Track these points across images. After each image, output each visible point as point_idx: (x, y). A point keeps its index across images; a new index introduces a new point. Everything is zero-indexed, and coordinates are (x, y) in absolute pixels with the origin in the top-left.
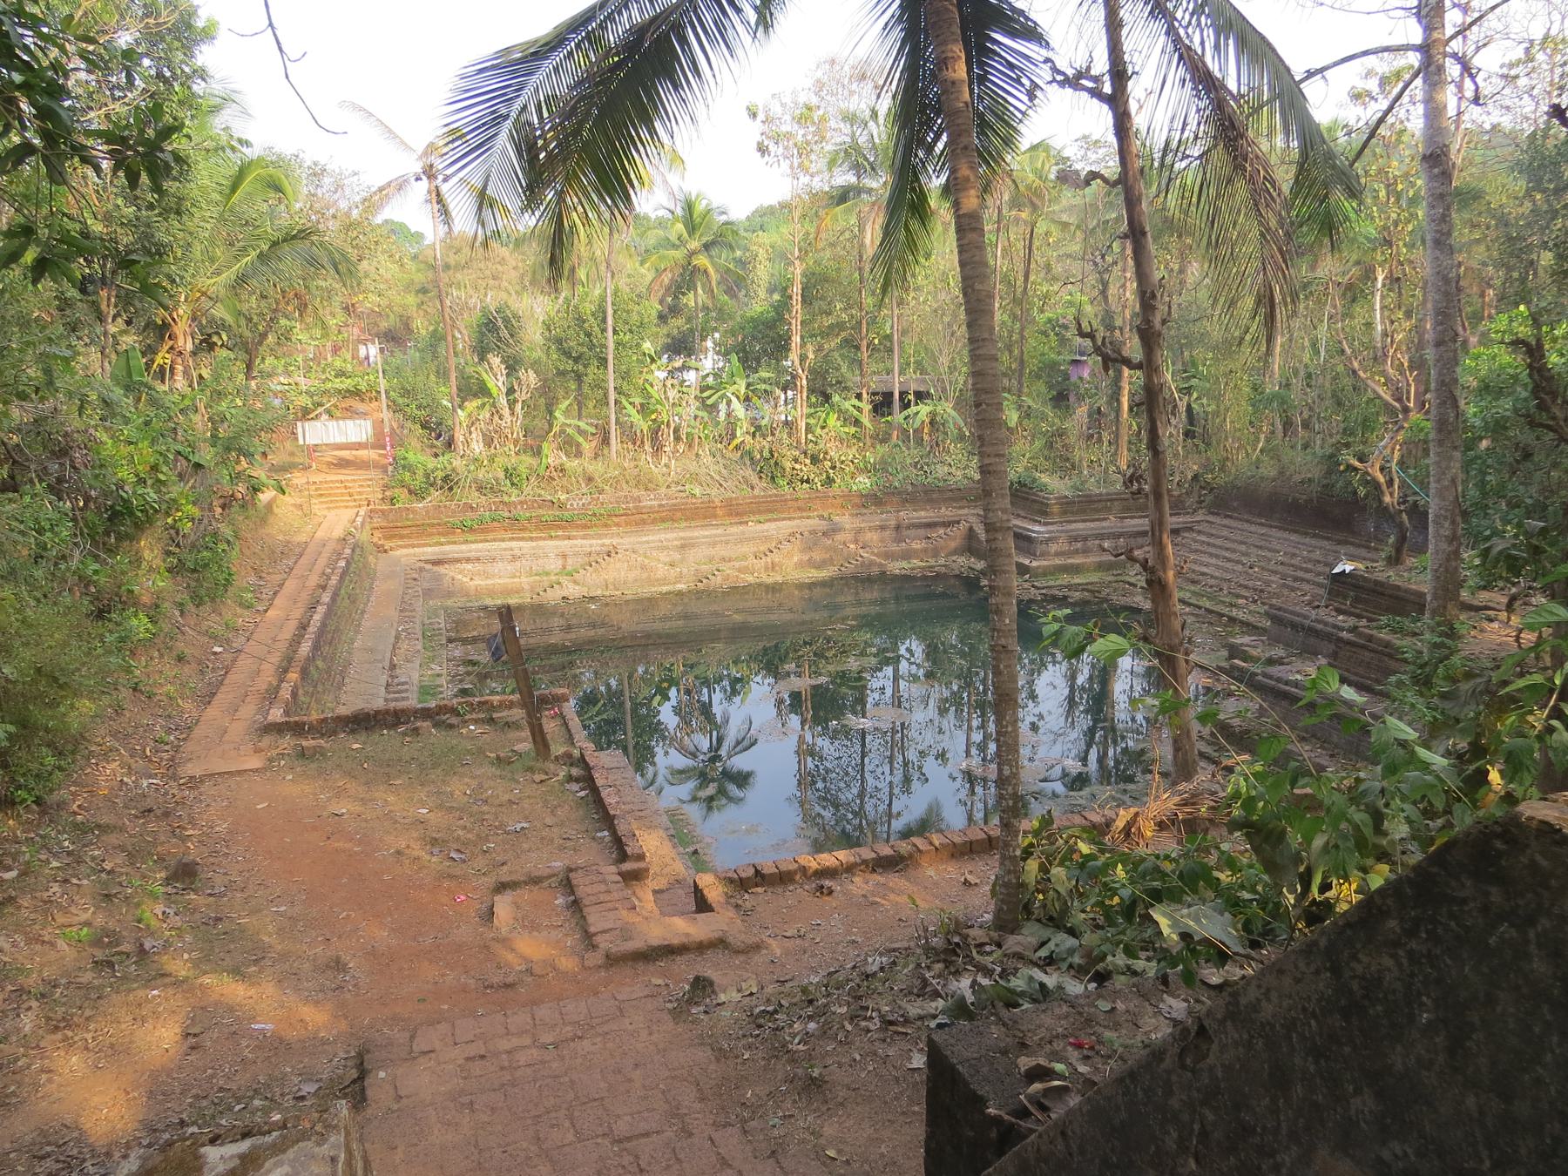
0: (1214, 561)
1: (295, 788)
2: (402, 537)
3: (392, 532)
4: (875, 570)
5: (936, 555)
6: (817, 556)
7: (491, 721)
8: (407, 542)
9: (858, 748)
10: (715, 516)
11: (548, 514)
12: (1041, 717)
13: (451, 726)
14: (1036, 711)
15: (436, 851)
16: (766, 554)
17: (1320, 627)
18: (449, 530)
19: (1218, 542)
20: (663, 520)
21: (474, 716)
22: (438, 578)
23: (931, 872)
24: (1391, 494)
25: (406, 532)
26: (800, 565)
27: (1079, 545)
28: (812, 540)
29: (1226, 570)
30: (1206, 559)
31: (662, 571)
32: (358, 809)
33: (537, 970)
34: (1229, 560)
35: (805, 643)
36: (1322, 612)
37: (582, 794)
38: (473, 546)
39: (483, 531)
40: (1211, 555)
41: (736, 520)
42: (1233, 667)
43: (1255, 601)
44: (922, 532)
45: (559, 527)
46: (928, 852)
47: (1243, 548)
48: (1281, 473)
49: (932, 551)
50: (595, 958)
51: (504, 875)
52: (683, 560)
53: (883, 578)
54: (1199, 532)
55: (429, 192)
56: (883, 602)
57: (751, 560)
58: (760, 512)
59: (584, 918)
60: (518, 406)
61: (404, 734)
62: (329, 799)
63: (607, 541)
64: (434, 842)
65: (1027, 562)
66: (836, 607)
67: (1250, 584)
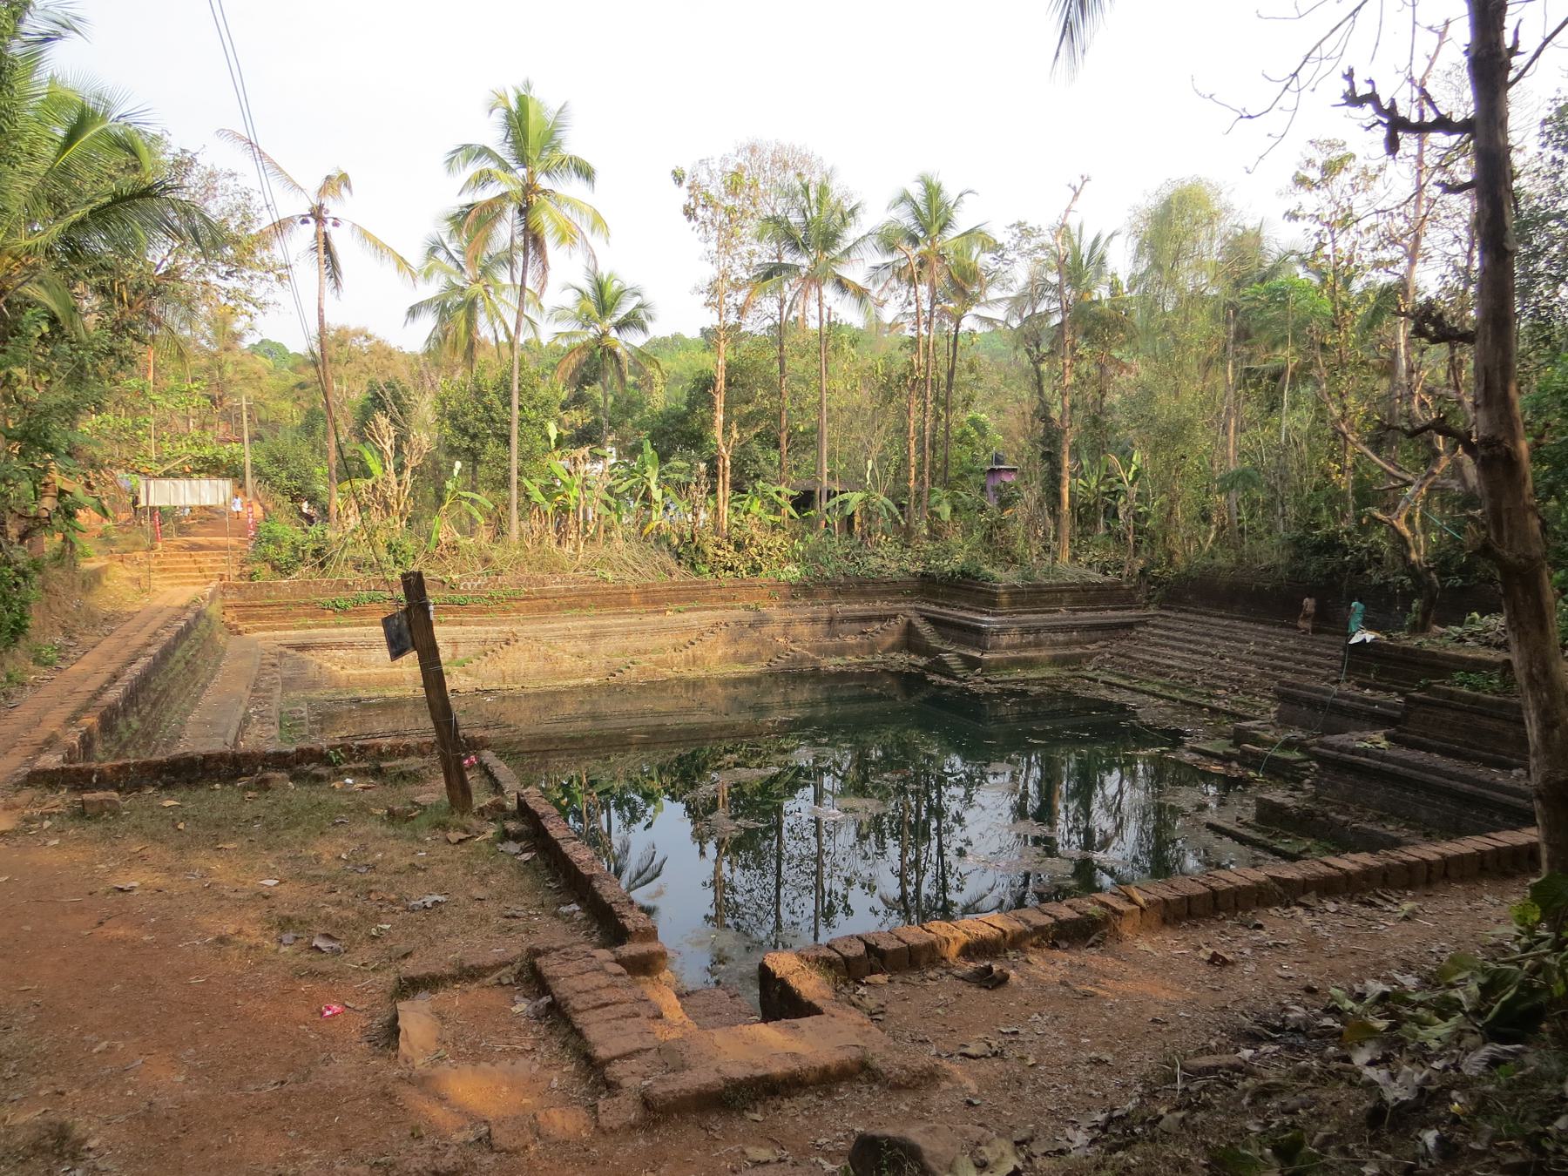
0: (1177, 653)
1: (61, 855)
2: (260, 618)
3: (248, 612)
4: (808, 666)
5: (872, 652)
6: (744, 648)
7: (378, 773)
8: (266, 623)
9: (771, 879)
10: (629, 604)
12: (969, 843)
13: (319, 779)
14: (963, 836)
15: (288, 937)
16: (689, 649)
17: (1346, 702)
18: (319, 611)
19: (1178, 635)
20: (570, 606)
21: (353, 766)
22: (302, 665)
23: (1143, 945)
24: (1418, 551)
26: (724, 659)
27: (1031, 637)
28: (739, 632)
29: (1195, 662)
30: (1169, 652)
31: (568, 663)
32: (159, 880)
33: (502, 1138)
34: (1194, 652)
35: (726, 751)
36: (1344, 687)
37: (526, 856)
38: (346, 630)
40: (1173, 648)
41: (653, 608)
42: (1245, 753)
43: (1235, 692)
44: (856, 626)
45: (450, 611)
46: (1131, 913)
47: (1208, 640)
48: (1240, 561)
49: (868, 647)
50: (620, 1111)
51: (411, 968)
52: (592, 651)
53: (816, 675)
54: (1155, 626)
55: (316, 236)
56: (813, 704)
57: (670, 653)
58: (680, 601)
59: (579, 1033)
60: (407, 474)
61: (246, 789)
62: (112, 871)
63: (506, 629)
64: (285, 923)
65: (978, 655)
66: (760, 709)
67: (1225, 674)
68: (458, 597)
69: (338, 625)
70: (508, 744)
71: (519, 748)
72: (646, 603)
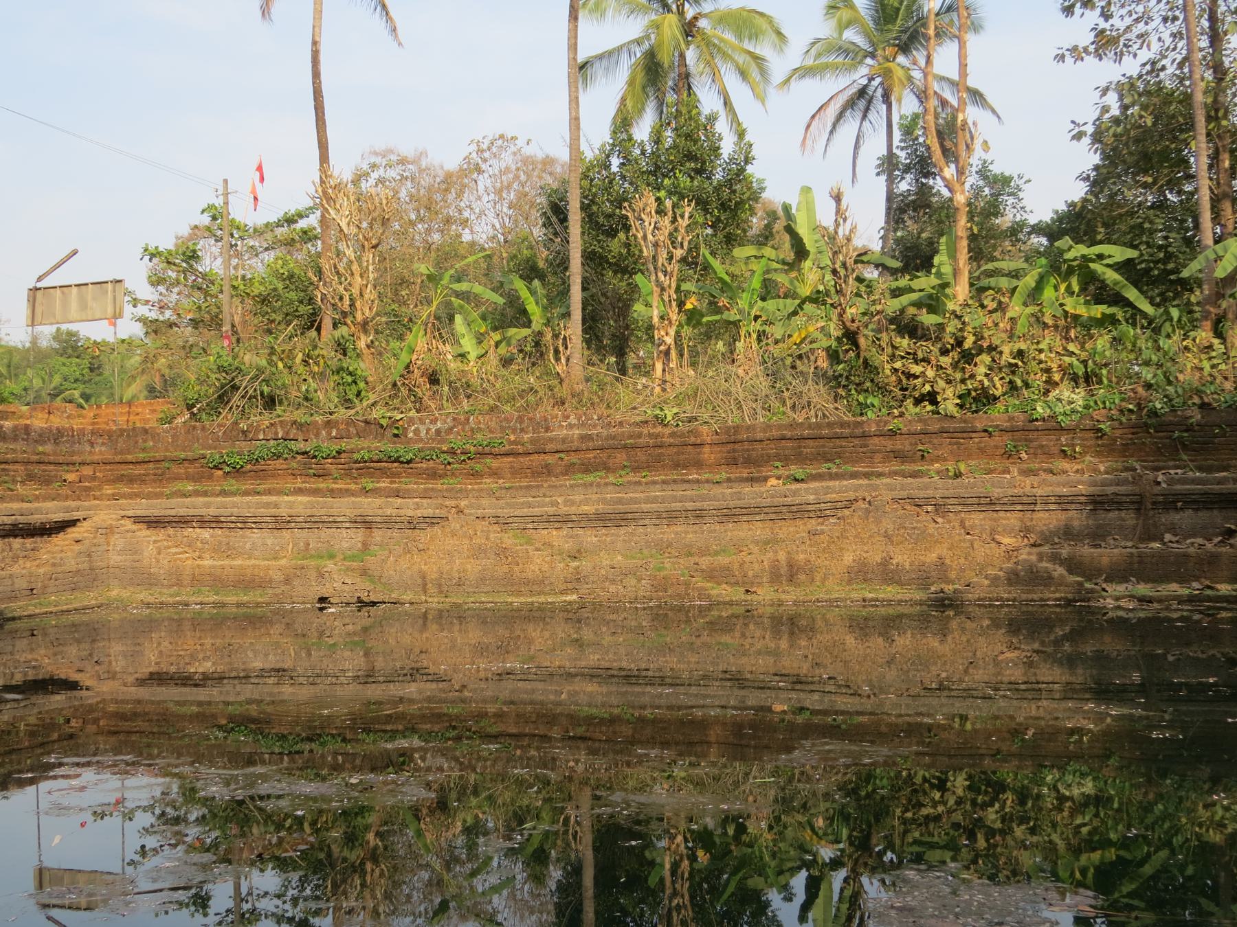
2: (131, 480)
10: (699, 465)
20: (587, 468)
25: (138, 470)
31: (537, 564)
39: (261, 475)
44: (1216, 517)
45: (384, 473)
58: (801, 459)
69: (224, 493)
70: (482, 715)
72: (732, 462)
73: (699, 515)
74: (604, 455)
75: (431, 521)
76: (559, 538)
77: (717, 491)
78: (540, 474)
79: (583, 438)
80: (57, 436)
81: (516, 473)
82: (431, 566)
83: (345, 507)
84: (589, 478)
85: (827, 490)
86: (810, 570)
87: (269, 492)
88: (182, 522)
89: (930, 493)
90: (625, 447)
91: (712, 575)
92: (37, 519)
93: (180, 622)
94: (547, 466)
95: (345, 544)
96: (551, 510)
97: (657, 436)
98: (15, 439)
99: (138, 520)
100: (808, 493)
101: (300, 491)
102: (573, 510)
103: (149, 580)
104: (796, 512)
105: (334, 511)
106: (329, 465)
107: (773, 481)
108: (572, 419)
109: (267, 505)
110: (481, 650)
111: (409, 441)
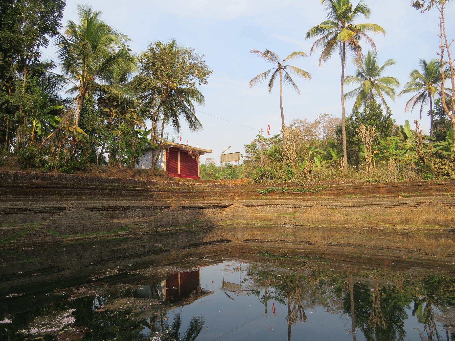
2: (242, 196)
10: (379, 193)
11: (295, 188)
20: (349, 193)
25: (244, 194)
31: (337, 217)
39: (270, 195)
45: (298, 195)
58: (408, 191)
68: (302, 189)
69: (262, 199)
70: (324, 254)
71: (328, 257)
72: (388, 192)
73: (380, 205)
74: (353, 190)
75: (310, 206)
76: (342, 211)
77: (384, 199)
78: (337, 195)
79: (348, 186)
80: (227, 186)
81: (331, 195)
82: (310, 217)
83: (289, 202)
84: (350, 196)
85: (416, 199)
86: (413, 221)
87: (272, 199)
88: (253, 205)
89: (448, 200)
90: (359, 188)
91: (384, 221)
92: (223, 204)
93: (253, 228)
94: (339, 193)
95: (290, 211)
96: (340, 204)
97: (368, 185)
98: (218, 187)
99: (244, 205)
100: (411, 200)
101: (279, 199)
102: (346, 204)
103: (246, 219)
104: (407, 205)
105: (287, 203)
106: (286, 192)
107: (400, 197)
108: (345, 182)
109: (272, 202)
110: (323, 238)
111: (304, 187)
